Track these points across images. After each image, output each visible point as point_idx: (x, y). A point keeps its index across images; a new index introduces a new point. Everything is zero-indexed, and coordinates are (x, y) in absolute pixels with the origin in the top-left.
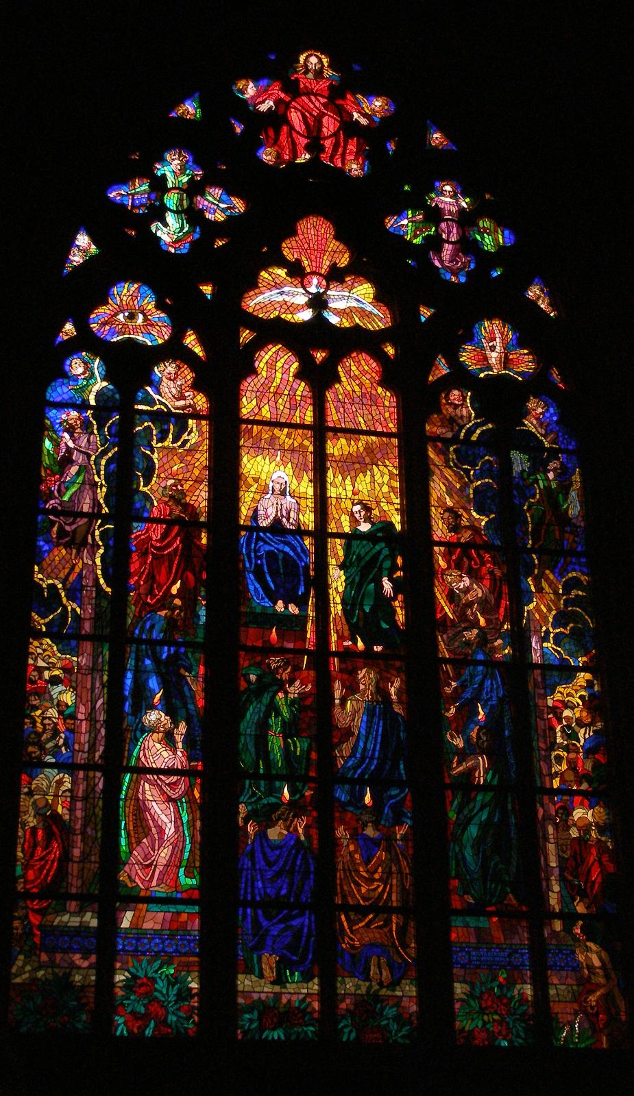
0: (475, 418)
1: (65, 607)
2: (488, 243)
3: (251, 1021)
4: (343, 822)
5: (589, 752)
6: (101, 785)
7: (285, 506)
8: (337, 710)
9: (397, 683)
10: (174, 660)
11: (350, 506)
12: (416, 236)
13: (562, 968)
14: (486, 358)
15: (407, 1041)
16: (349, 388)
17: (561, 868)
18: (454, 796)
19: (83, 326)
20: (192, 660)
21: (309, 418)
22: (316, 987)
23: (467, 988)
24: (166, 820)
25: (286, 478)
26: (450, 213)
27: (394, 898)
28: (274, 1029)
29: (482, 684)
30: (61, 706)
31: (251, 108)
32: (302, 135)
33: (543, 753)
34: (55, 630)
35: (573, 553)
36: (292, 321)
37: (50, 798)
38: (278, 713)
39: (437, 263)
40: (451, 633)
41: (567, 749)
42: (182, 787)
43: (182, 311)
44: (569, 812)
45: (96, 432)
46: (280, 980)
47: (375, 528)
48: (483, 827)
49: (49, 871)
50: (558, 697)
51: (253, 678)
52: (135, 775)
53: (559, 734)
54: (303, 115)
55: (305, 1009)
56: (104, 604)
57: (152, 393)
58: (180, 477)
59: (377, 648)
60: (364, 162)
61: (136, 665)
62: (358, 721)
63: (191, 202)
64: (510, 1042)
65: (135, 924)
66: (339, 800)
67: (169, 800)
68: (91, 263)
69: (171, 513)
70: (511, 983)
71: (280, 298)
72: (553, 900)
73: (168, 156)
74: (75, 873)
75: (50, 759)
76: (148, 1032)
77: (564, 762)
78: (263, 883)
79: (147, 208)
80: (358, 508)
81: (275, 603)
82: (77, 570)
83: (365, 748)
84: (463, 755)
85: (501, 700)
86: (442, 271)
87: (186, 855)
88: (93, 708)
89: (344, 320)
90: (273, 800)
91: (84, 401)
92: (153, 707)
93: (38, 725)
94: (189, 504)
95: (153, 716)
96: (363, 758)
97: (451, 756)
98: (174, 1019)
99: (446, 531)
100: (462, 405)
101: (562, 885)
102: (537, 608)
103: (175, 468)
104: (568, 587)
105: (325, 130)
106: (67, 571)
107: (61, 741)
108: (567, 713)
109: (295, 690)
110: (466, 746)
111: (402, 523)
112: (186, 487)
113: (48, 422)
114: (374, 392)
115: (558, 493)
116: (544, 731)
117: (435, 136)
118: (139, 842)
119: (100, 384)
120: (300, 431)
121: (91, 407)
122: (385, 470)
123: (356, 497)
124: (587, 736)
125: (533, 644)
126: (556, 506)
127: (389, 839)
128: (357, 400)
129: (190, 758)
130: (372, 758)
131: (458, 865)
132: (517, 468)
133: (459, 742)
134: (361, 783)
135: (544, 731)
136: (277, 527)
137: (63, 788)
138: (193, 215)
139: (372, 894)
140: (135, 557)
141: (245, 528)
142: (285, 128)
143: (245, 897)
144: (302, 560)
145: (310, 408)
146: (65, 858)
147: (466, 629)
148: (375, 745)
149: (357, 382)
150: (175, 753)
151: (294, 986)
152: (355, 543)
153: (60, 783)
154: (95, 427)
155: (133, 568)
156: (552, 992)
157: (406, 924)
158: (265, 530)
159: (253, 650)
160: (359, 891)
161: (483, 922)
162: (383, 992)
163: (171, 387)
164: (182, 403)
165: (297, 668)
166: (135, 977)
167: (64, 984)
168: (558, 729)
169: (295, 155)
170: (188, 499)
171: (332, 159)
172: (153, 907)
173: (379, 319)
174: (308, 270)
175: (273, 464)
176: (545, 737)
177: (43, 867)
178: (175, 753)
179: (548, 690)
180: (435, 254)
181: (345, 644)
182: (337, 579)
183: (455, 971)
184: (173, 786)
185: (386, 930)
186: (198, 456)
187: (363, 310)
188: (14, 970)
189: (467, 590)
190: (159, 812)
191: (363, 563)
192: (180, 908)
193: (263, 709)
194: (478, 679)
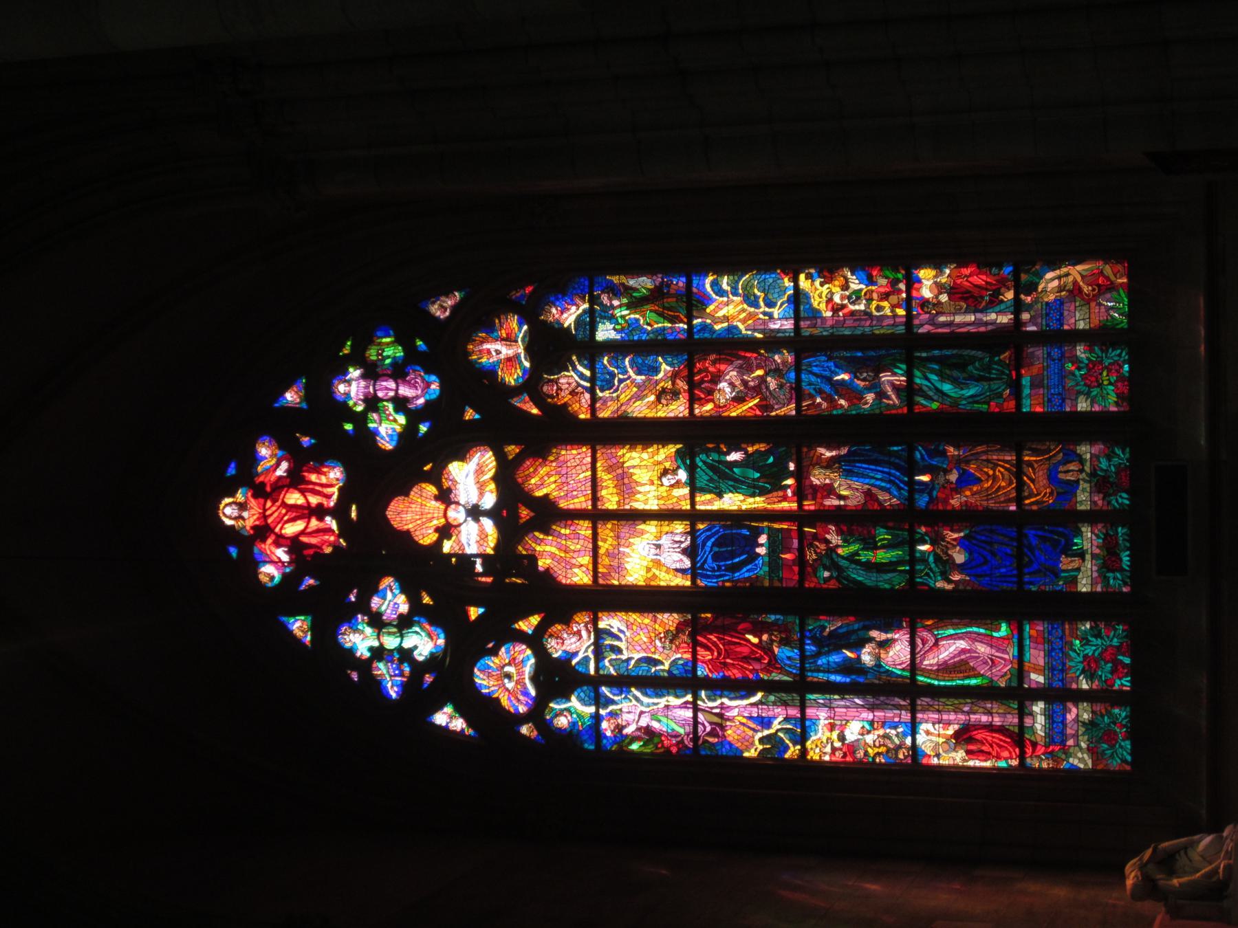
1: (778, 731)
3: (1114, 578)
4: (946, 501)
5: (871, 281)
8: (849, 503)
9: (821, 450)
11: (664, 489)
12: (395, 421)
13: (1062, 315)
14: (509, 359)
16: (553, 486)
17: (974, 312)
18: (918, 403)
21: (587, 524)
23: (1081, 398)
26: (367, 387)
28: (1121, 560)
30: (863, 732)
31: (288, 570)
32: (308, 523)
34: (798, 738)
36: (495, 536)
37: (941, 740)
38: (857, 553)
39: (421, 401)
40: (772, 402)
41: (870, 300)
43: (498, 631)
44: (924, 303)
46: (1081, 555)
48: (943, 378)
50: (823, 306)
51: (826, 574)
53: (857, 307)
54: (287, 522)
56: (772, 698)
59: (792, 467)
61: (824, 672)
62: (857, 485)
63: (389, 624)
64: (1125, 362)
66: (928, 503)
67: (936, 644)
68: (461, 711)
70: (1076, 361)
72: (1005, 319)
75: (908, 741)
76: (1127, 660)
81: (759, 555)
82: (744, 721)
84: (881, 395)
85: (830, 358)
86: (427, 397)
87: (982, 631)
88: (863, 706)
90: (931, 559)
92: (859, 658)
96: (890, 482)
99: (678, 403)
102: (744, 321)
104: (721, 293)
107: (893, 732)
108: (837, 299)
109: (834, 539)
112: (661, 630)
118: (973, 669)
119: (574, 703)
121: (597, 711)
122: (628, 455)
127: (958, 462)
128: (564, 479)
129: (900, 628)
131: (977, 402)
132: (613, 335)
133: (870, 397)
134: (912, 483)
137: (932, 730)
138: (404, 623)
139: (1007, 477)
140: (728, 673)
142: (304, 539)
144: (717, 532)
146: (990, 728)
147: (767, 388)
150: (894, 641)
152: (698, 484)
153: (928, 733)
155: (739, 675)
156: (1081, 325)
157: (1030, 449)
158: (694, 563)
159: (802, 575)
160: (1004, 488)
161: (1026, 381)
162: (1087, 468)
163: (573, 643)
164: (584, 633)
165: (815, 537)
166: (1083, 672)
167: (1091, 725)
168: (852, 307)
169: (329, 531)
171: (329, 497)
172: (1027, 656)
173: (486, 459)
174: (443, 521)
176: (860, 320)
178: (894, 641)
182: (732, 501)
183: (1068, 409)
184: (924, 642)
187: (476, 471)
189: (732, 385)
191: (715, 477)
192: (1026, 635)
194: (813, 379)
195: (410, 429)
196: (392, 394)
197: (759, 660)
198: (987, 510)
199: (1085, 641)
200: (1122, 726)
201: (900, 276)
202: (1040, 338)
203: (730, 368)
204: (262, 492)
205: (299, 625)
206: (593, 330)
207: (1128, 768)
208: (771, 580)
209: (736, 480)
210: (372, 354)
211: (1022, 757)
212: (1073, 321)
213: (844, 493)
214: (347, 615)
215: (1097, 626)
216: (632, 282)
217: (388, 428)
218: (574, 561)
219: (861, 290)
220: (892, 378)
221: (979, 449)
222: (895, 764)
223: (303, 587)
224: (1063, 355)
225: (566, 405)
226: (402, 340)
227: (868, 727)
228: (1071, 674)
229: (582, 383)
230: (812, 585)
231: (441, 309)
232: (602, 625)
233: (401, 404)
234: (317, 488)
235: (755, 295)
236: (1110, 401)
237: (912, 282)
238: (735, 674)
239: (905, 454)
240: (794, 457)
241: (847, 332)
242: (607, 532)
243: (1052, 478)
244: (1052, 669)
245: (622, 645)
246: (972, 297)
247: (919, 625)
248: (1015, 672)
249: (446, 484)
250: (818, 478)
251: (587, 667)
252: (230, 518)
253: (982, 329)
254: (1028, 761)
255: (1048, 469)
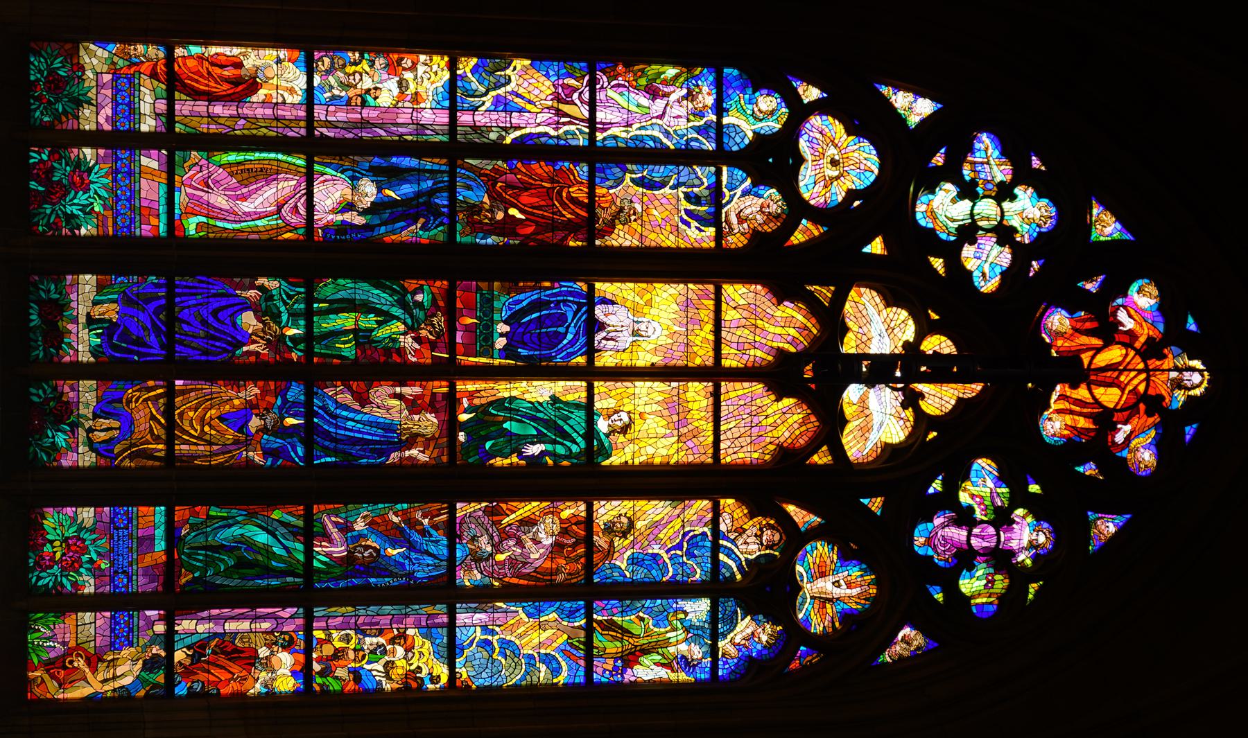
0: (746, 560)
1: (485, 94)
2: (970, 585)
4: (264, 392)
5: (356, 674)
6: (291, 134)
7: (619, 334)
8: (390, 390)
9: (423, 458)
10: (434, 211)
11: (627, 409)
12: (973, 496)
13: (113, 630)
14: (823, 575)
15: (31, 456)
16: (770, 411)
18: (298, 517)
19: (817, 107)
20: (435, 231)
21: (726, 363)
22: (85, 359)
23: (89, 523)
24: (257, 202)
25: (653, 337)
26: (1008, 539)
27: (183, 447)
28: (39, 315)
29: (430, 555)
31: (1120, 301)
32: (1090, 363)
33: (353, 621)
34: (459, 83)
35: (589, 670)
37: (274, 81)
38: (379, 323)
39: (938, 521)
40: (486, 520)
42: (294, 220)
43: (846, 221)
44: (289, 646)
45: (691, 124)
47: (603, 437)
48: (267, 549)
49: (197, 81)
50: (419, 641)
51: (419, 297)
52: (303, 170)
53: (375, 640)
54: (1120, 363)
55: (61, 348)
56: (493, 136)
57: (743, 186)
58: (645, 218)
59: (462, 437)
60: (1063, 436)
62: (379, 413)
63: (987, 231)
65: (142, 171)
69: (603, 208)
70: (96, 572)
71: (874, 333)
72: (186, 625)
73: (1045, 201)
74: (196, 108)
75: (317, 80)
76: (33, 185)
77: (343, 645)
78: (195, 306)
79: (973, 180)
80: (626, 419)
81: (506, 322)
82: (529, 107)
83: (347, 419)
84: (345, 528)
85: (410, 575)
86: (930, 526)
89: (855, 407)
90: (284, 318)
91: (727, 111)
92: (380, 190)
93: (353, 68)
94: (614, 228)
95: (369, 189)
96: (336, 417)
97: (343, 515)
98: (48, 211)
99: (606, 518)
100: (762, 544)
101: (203, 636)
102: (519, 622)
103: (654, 212)
104: (548, 659)
105: (1101, 390)
106: (526, 95)
107: (336, 92)
108: (400, 651)
109: (407, 342)
110: (355, 533)
111: (611, 466)
112: (634, 225)
113: (697, 72)
114: (768, 440)
115: (663, 655)
116: (377, 624)
117: (1111, 525)
118: (232, 175)
120: (711, 354)
121: (720, 117)
122: (672, 451)
123: (637, 416)
124: (374, 673)
125: (477, 616)
126: (646, 651)
127: (248, 441)
128: (756, 420)
129: (325, 229)
130: (337, 427)
132: (688, 605)
133: (360, 526)
134: (309, 414)
135: (377, 624)
136: (594, 326)
137: (286, 95)
138: (968, 233)
141: (591, 288)
142: (1096, 342)
143: (178, 286)
145: (740, 365)
146: (211, 98)
147: (491, 537)
148: (351, 430)
149: (779, 421)
151: (86, 337)
152: (582, 413)
153: (292, 91)
154: (697, 124)
155: (534, 165)
156: (88, 617)
158: (591, 312)
159: (450, 296)
160: (190, 409)
161: (160, 545)
162: (82, 433)
163: (750, 206)
164: (734, 220)
165: (433, 346)
168: (381, 640)
170: (620, 227)
171: (1063, 397)
172: (163, 190)
173: (857, 446)
175: (670, 323)
177: (202, 76)
178: (333, 211)
179: (425, 630)
180: (950, 519)
181: (465, 400)
182: (538, 391)
183: (106, 509)
185: (149, 437)
186: (672, 237)
188: (92, 47)
189: (536, 542)
190: (265, 196)
191: (561, 423)
192: (163, 218)
193: (385, 308)
194: (432, 549)
195: (952, 489)
196: (976, 531)
197: (509, 186)
198: (212, 380)
199: (89, 210)
200: (39, 99)
201: (319, 680)
202: (141, 602)
203: (538, 563)
204: (1153, 403)
205: (1106, 227)
206: (714, 611)
207: (33, 45)
208: (491, 289)
209: (534, 419)
210: (1001, 583)
211: (170, 59)
212: (99, 623)
213: (395, 402)
214: (1043, 243)
215: (71, 230)
216: (663, 673)
217: (982, 485)
218: (745, 314)
219: (369, 663)
220: (331, 550)
221: (221, 459)
222: (335, 50)
223: (1100, 278)
224: (112, 580)
225: (752, 516)
226: (959, 601)
227: (369, 98)
228: (106, 168)
229: (729, 545)
230: (438, 284)
231: (909, 638)
232: (711, 231)
233: (964, 518)
234: (1078, 409)
235: (505, 657)
236: (54, 522)
237: (304, 672)
238: (541, 168)
239: (317, 453)
240: (458, 448)
241: (387, 609)
242: (701, 352)
243: (128, 423)
244: (130, 174)
245: (684, 205)
246: (226, 654)
247: (301, 231)
248: (178, 170)
249: (909, 413)
250: (428, 423)
251: (730, 176)
252: (1193, 369)
253: (215, 612)
254: (161, 55)
255: (132, 433)
